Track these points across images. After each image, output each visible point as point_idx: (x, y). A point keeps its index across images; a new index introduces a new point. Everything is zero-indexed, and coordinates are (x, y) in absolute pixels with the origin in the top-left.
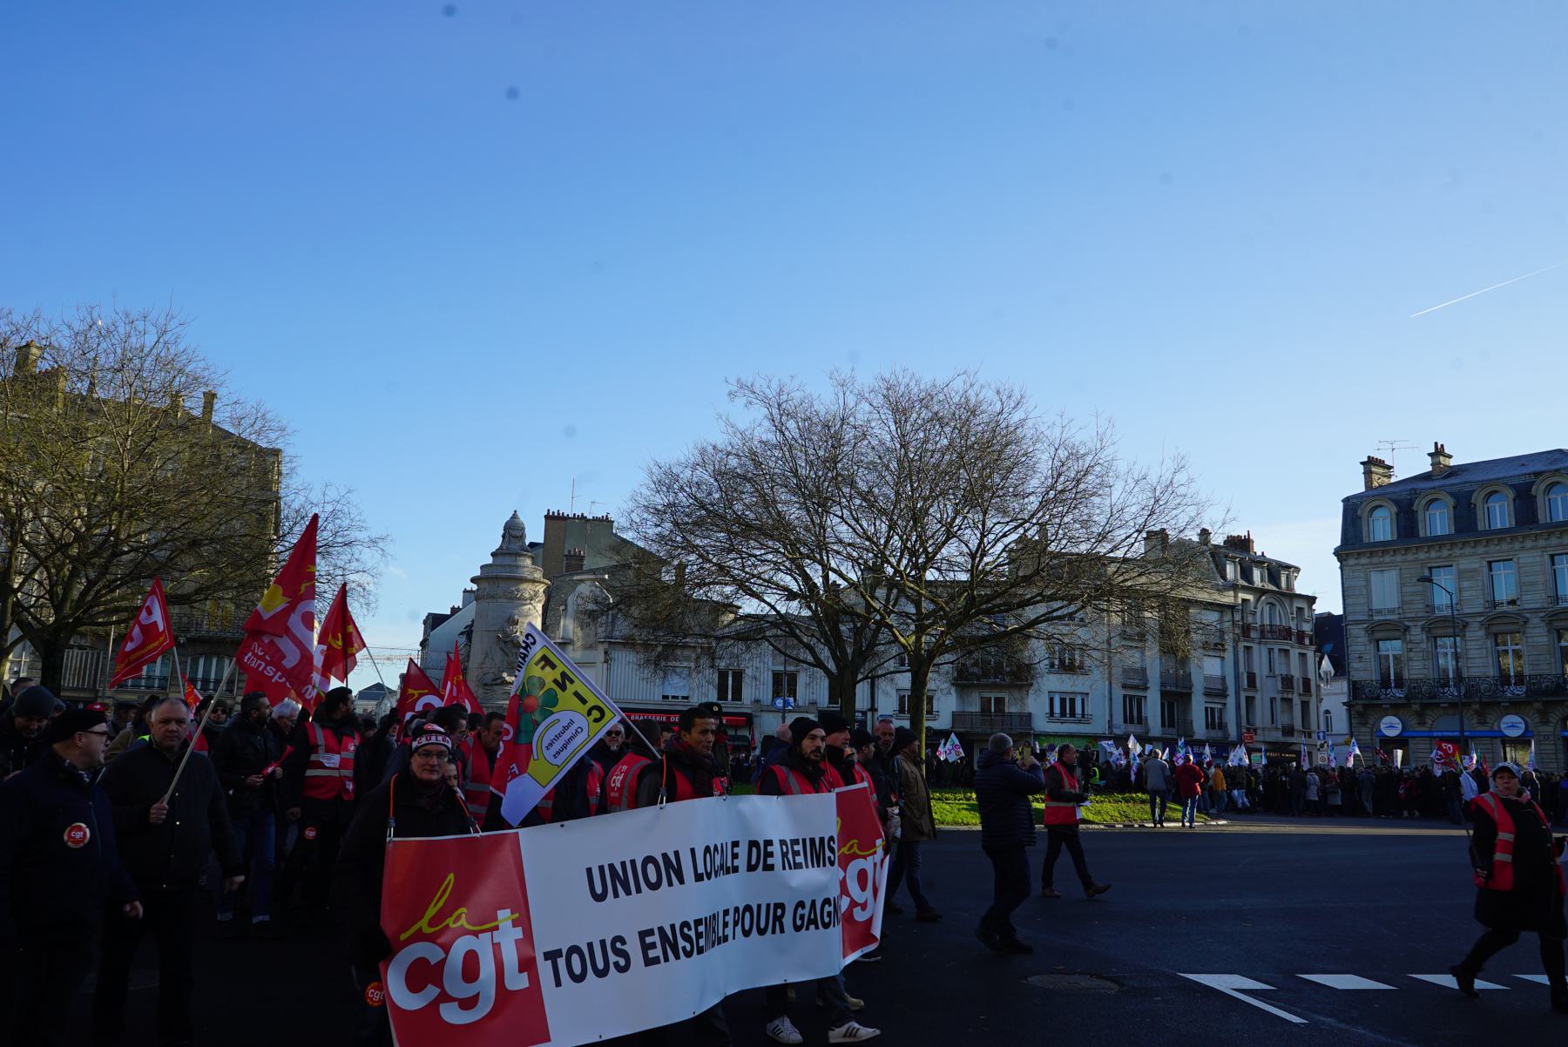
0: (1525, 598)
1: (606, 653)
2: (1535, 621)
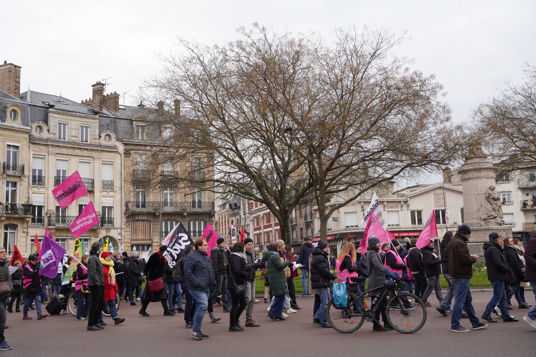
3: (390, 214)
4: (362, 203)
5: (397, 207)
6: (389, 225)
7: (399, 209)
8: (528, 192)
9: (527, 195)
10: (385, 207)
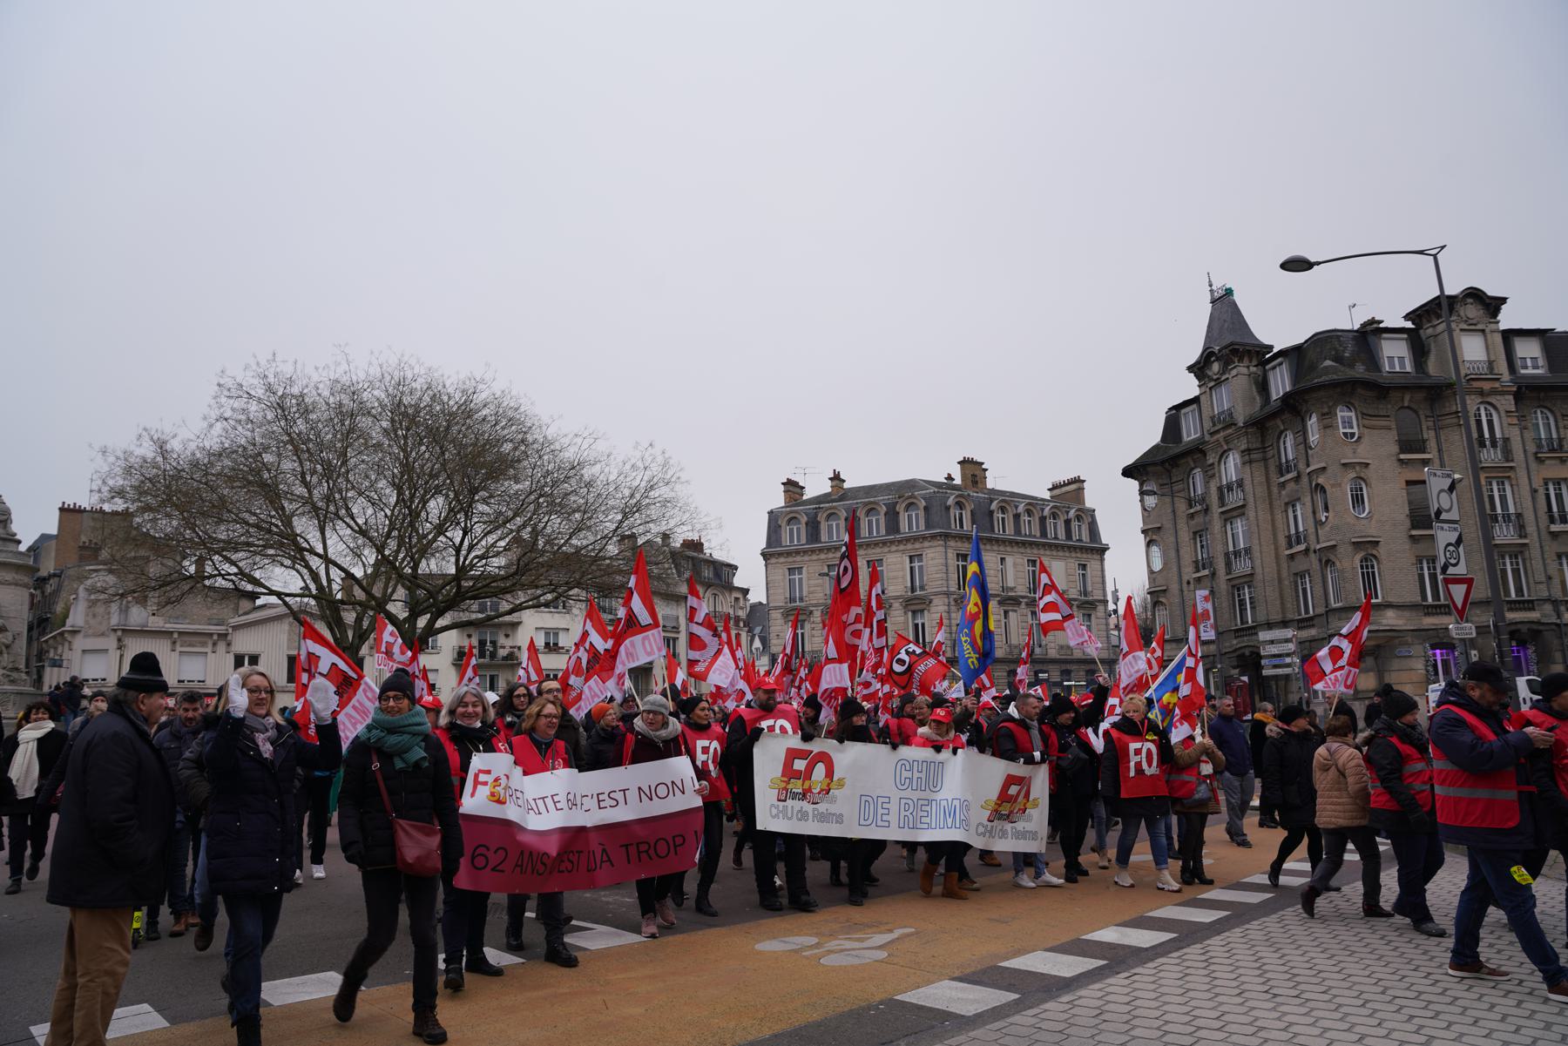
0: (891, 588)
1: (119, 640)
2: (896, 605)
3: (185, 659)
4: (119, 633)
5: (204, 644)
6: (179, 681)
7: (209, 649)
8: (471, 630)
9: (469, 636)
10: (174, 643)
